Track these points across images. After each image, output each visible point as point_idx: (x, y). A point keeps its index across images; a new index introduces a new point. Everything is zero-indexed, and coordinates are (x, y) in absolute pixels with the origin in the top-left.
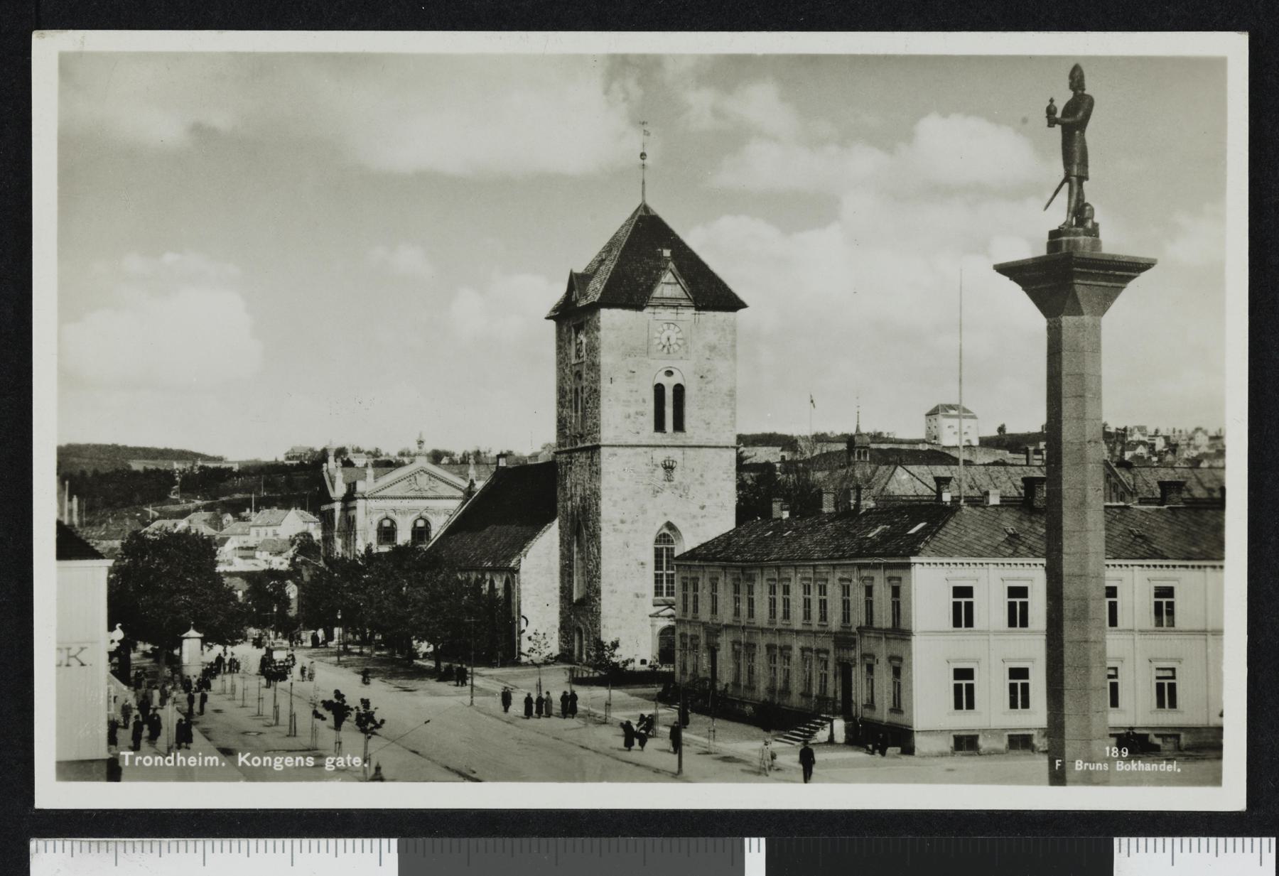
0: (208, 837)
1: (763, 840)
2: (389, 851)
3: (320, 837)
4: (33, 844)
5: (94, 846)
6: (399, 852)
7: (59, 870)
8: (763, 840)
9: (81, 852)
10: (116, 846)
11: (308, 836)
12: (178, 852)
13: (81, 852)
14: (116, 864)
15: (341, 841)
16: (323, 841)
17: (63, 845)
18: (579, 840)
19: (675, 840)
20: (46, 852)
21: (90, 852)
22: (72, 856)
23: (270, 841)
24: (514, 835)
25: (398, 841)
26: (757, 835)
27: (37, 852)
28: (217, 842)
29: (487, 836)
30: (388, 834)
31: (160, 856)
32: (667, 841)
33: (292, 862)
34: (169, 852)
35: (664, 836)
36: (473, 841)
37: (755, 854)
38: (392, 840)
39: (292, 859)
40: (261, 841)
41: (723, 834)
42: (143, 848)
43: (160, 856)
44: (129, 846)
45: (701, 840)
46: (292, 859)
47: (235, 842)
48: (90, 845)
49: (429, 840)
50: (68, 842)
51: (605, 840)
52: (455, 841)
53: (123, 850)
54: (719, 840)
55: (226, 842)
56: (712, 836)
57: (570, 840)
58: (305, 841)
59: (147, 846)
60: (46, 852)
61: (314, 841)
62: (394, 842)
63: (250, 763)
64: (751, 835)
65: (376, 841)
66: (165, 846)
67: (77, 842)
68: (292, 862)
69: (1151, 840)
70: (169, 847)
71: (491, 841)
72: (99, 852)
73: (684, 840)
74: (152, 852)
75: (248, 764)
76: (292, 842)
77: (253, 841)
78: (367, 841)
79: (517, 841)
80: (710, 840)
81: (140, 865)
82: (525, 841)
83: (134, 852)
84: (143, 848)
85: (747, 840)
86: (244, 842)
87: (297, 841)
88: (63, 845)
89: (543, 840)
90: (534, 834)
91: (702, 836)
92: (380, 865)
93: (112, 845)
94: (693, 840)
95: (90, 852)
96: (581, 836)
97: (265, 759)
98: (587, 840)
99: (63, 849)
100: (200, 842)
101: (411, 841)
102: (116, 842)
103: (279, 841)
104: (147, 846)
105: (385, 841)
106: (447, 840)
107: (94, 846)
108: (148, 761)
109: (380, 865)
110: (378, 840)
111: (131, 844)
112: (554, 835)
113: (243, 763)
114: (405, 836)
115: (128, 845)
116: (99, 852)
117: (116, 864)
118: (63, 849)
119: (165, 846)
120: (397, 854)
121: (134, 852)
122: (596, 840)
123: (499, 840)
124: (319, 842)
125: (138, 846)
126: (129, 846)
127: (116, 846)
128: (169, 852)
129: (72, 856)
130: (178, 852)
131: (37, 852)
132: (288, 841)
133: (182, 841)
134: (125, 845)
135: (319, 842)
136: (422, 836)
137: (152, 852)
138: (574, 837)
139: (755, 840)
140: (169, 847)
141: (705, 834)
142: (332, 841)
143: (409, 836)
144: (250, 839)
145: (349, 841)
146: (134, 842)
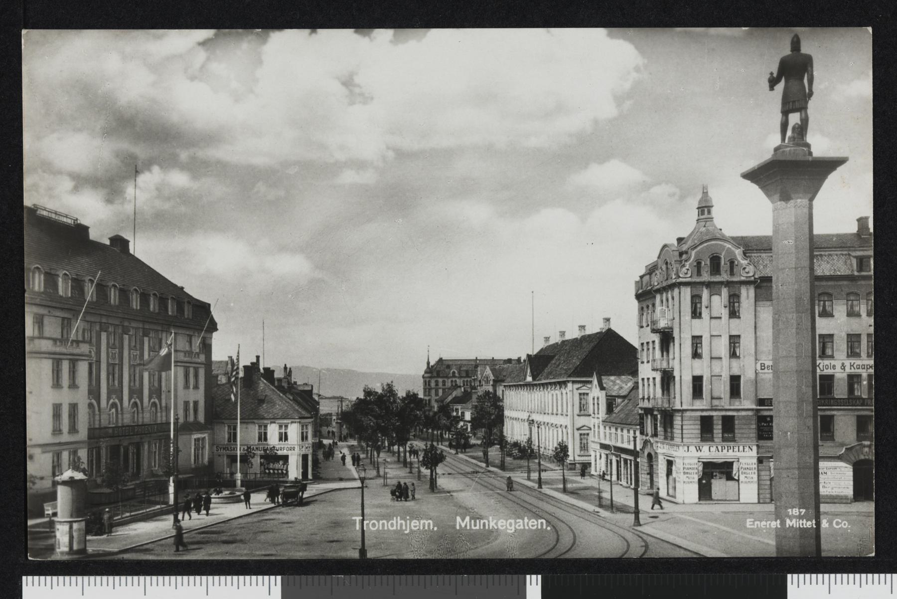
1: (540, 577)
8: (540, 577)
26: (536, 573)
30: (275, 574)
37: (534, 587)
62: (279, 578)
63: (497, 526)
64: (531, 573)
75: (496, 528)
85: (528, 577)
92: (269, 594)
97: (381, 522)
101: (291, 577)
105: (273, 577)
108: (374, 525)
109: (269, 594)
113: (493, 526)
139: (534, 577)
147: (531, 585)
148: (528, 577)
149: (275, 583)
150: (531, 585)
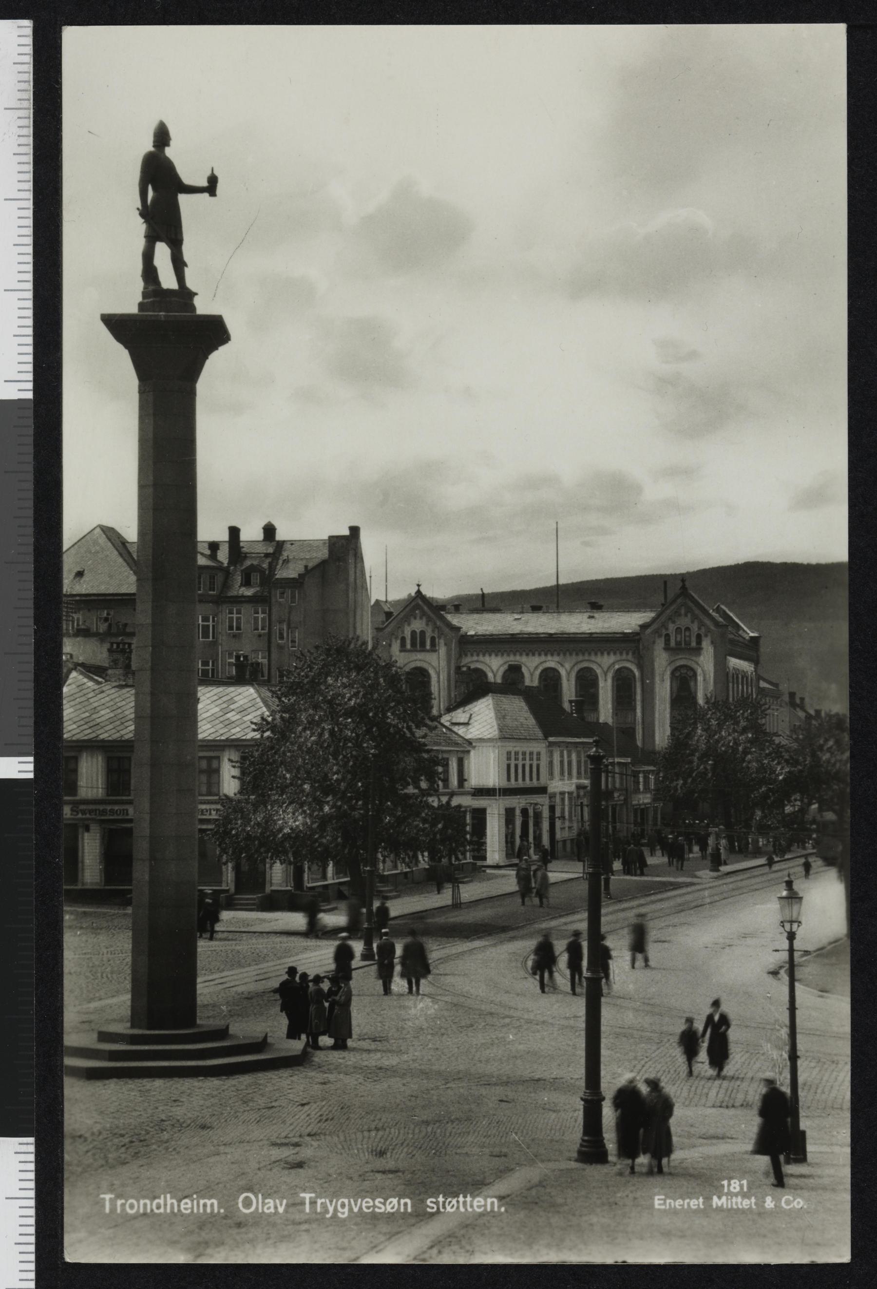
0: (34, 203)
1: (31, 776)
2: (19, 390)
3: (34, 320)
4: (25, 26)
6: (19, 400)
8: (31, 776)
9: (19, 72)
10: (25, 109)
12: (19, 172)
13: (19, 72)
14: (6, 109)
17: (26, 54)
18: (31, 586)
20: (19, 36)
21: (19, 82)
22: (14, 63)
23: (30, 268)
24: (36, 520)
25: (29, 400)
26: (36, 770)
27: (18, 27)
28: (30, 213)
30: (36, 390)
31: (14, 154)
32: (31, 676)
33: (8, 290)
34: (19, 163)
35: (35, 673)
36: (30, 477)
39: (12, 290)
40: (30, 259)
41: (37, 734)
42: (23, 136)
43: (14, 154)
45: (31, 712)
46: (12, 290)
47: (30, 231)
48: (25, 82)
49: (31, 431)
51: (31, 613)
52: (30, 458)
54: (31, 731)
55: (30, 222)
56: (35, 723)
57: (31, 577)
58: (30, 304)
59: (24, 141)
60: (19, 36)
61: (30, 313)
62: (29, 395)
64: (36, 763)
65: (30, 377)
68: (8, 290)
70: (23, 163)
71: (31, 495)
72: (19, 91)
73: (31, 694)
74: (19, 145)
76: (29, 290)
77: (30, 249)
78: (30, 367)
79: (31, 522)
80: (31, 722)
81: (5, 134)
82: (30, 530)
83: (19, 127)
84: (23, 136)
85: (31, 759)
86: (30, 240)
87: (30, 295)
88: (26, 54)
92: (6, 381)
94: (31, 704)
95: (19, 82)
96: (36, 589)
98: (31, 594)
99: (22, 54)
100: (30, 195)
101: (30, 413)
103: (30, 277)
104: (24, 141)
105: (30, 386)
106: (30, 449)
109: (6, 381)
111: (27, 124)
112: (36, 561)
114: (35, 406)
116: (19, 91)
117: (6, 109)
118: (22, 54)
120: (16, 398)
121: (19, 127)
122: (31, 604)
123: (30, 504)
124: (29, 318)
127: (25, 109)
128: (19, 163)
129: (14, 63)
130: (19, 172)
131: (18, 27)
132: (30, 286)
134: (26, 118)
135: (29, 318)
136: (35, 423)
137: (19, 145)
138: (35, 582)
139: (31, 767)
140: (23, 163)
141: (37, 715)
143: (35, 412)
148: (31, 759)
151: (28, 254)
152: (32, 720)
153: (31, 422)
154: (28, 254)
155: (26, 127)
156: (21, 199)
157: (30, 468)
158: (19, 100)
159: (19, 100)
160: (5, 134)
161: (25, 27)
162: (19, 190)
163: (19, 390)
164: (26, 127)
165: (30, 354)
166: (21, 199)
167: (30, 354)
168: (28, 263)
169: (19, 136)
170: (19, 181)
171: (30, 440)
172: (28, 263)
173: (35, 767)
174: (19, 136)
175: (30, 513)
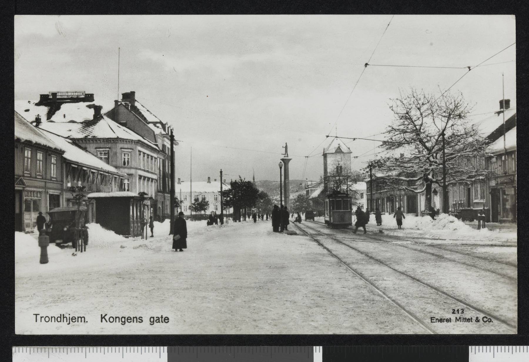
0: (87, 346)
1: (321, 347)
2: (164, 352)
4: (14, 349)
5: (39, 350)
6: (168, 352)
7: (24, 360)
8: (321, 347)
10: (49, 350)
11: (130, 346)
12: (75, 352)
14: (49, 357)
15: (143, 348)
16: (136, 348)
17: (26, 349)
19: (284, 347)
20: (19, 352)
21: (38, 352)
24: (216, 345)
28: (91, 348)
29: (205, 345)
30: (163, 345)
31: (67, 354)
32: (281, 347)
36: (199, 348)
37: (318, 353)
38: (165, 347)
39: (123, 355)
40: (110, 348)
41: (304, 344)
42: (60, 350)
43: (67, 354)
44: (54, 350)
46: (123, 355)
47: (99, 348)
48: (38, 349)
49: (180, 347)
50: (28, 348)
51: (255, 347)
52: (191, 348)
53: (51, 351)
54: (303, 347)
55: (95, 348)
56: (300, 346)
57: (240, 347)
58: (128, 348)
59: (62, 350)
60: (19, 352)
61: (132, 348)
62: (166, 348)
65: (158, 348)
66: (69, 350)
67: (32, 348)
69: (507, 347)
70: (71, 350)
71: (206, 348)
72: (41, 352)
73: (288, 347)
74: (64, 352)
77: (106, 348)
78: (154, 348)
79: (218, 347)
82: (221, 347)
83: (56, 352)
84: (60, 350)
85: (314, 347)
86: (102, 348)
87: (125, 348)
88: (26, 349)
89: (229, 347)
90: (225, 345)
91: (295, 346)
93: (47, 349)
94: (292, 347)
95: (38, 352)
96: (245, 345)
98: (247, 347)
99: (26, 351)
100: (84, 348)
101: (173, 347)
102: (49, 348)
103: (117, 348)
104: (62, 350)
105: (162, 348)
106: (188, 347)
107: (39, 350)
110: (159, 347)
111: (55, 349)
114: (170, 346)
115: (53, 349)
116: (41, 352)
117: (49, 357)
118: (26, 351)
119: (69, 350)
120: (167, 353)
121: (56, 352)
122: (251, 347)
123: (210, 347)
125: (58, 350)
126: (54, 350)
127: (49, 350)
130: (75, 352)
132: (121, 348)
133: (76, 348)
136: (177, 346)
137: (64, 352)
139: (318, 347)
140: (71, 350)
141: (297, 345)
142: (140, 348)
144: (105, 347)
145: (147, 348)
146: (56, 348)
147: (316, 352)
149: (163, 351)
150: (316, 352)
151: (108, 349)
152: (298, 347)
153: (177, 347)
154: (108, 349)
155: (56, 350)
156: (86, 351)
157: (195, 348)
158: (45, 352)
159: (45, 352)
160: (59, 358)
161: (15, 349)
162: (82, 352)
163: (164, 352)
164: (56, 350)
165: (149, 348)
166: (86, 351)
167: (149, 348)
168: (112, 348)
169: (60, 352)
170: (78, 352)
171: (184, 347)
172: (112, 348)
173: (317, 346)
174: (60, 352)
175: (214, 347)
